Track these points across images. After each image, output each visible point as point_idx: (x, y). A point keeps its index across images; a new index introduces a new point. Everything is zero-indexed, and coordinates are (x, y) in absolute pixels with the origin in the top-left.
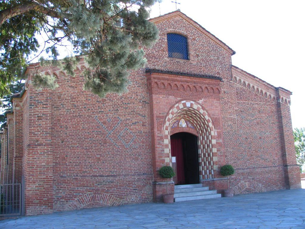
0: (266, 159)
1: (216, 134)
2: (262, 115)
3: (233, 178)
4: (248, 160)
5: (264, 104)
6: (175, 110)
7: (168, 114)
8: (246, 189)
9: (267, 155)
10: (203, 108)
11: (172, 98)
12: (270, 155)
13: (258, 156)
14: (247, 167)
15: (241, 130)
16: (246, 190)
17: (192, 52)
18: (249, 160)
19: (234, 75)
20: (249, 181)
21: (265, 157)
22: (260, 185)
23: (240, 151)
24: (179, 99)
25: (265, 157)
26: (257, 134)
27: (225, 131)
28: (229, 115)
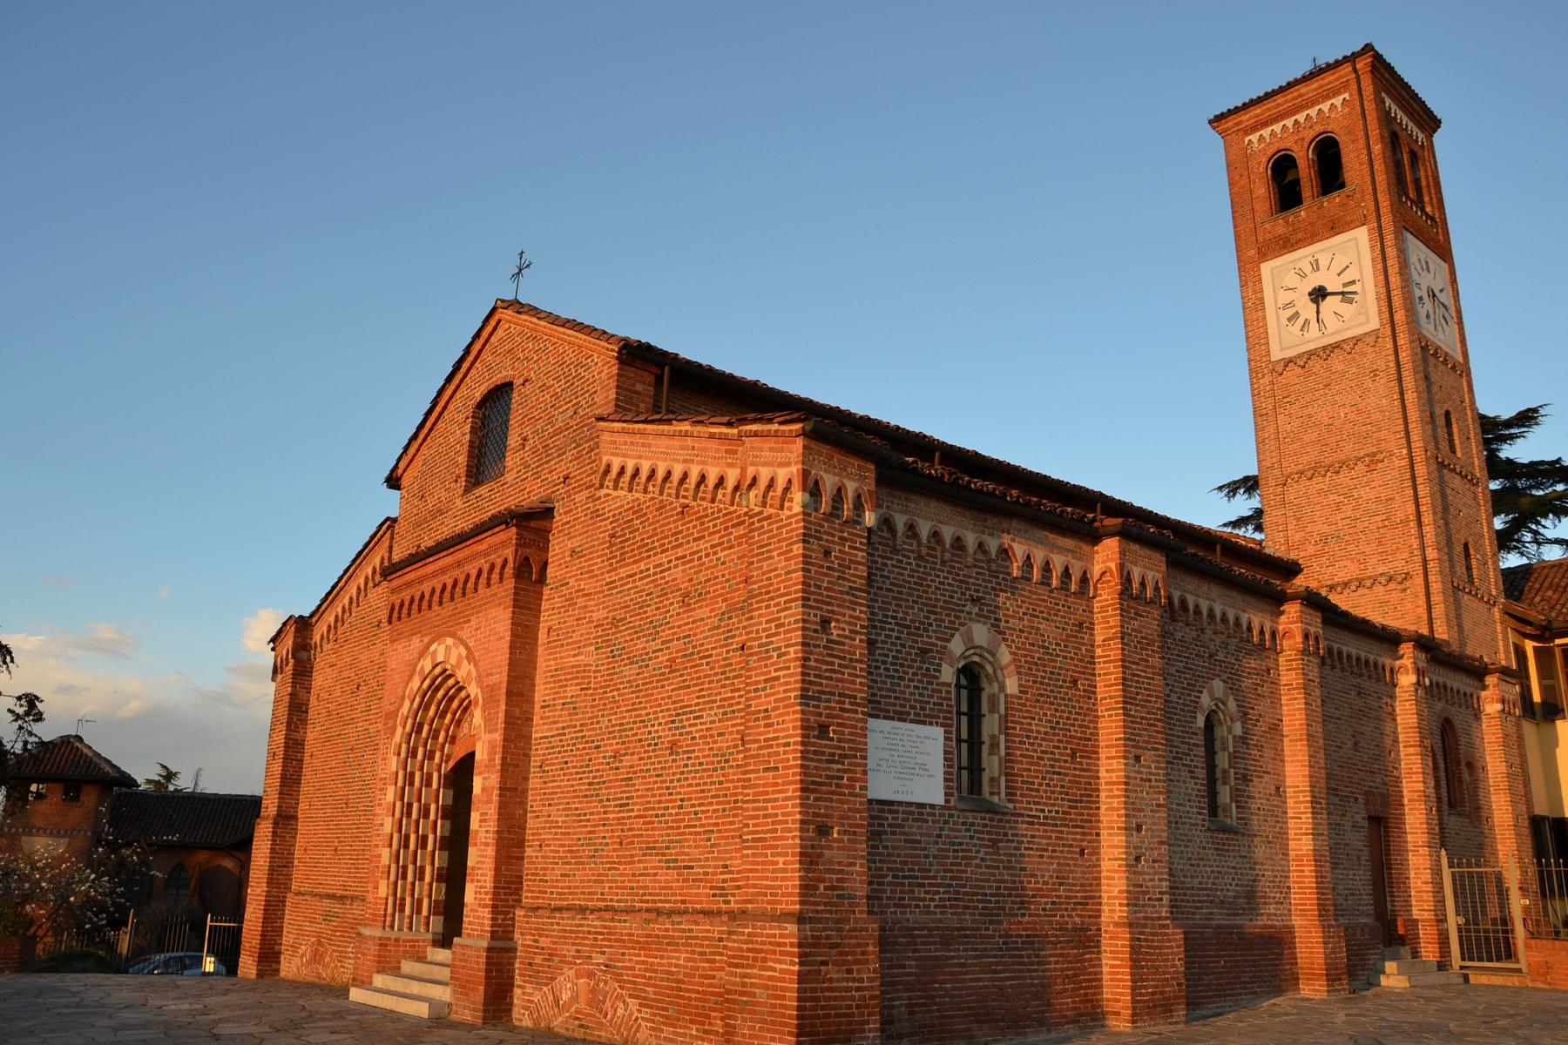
0: (686, 867)
1: (485, 757)
2: (700, 613)
3: (543, 948)
4: (610, 869)
5: (713, 546)
6: (416, 683)
7: (403, 698)
8: (576, 1012)
9: (695, 841)
10: (470, 657)
11: (416, 643)
12: (709, 840)
13: (650, 849)
14: (605, 900)
15: (603, 716)
16: (577, 1019)
17: (513, 441)
18: (616, 869)
19: (606, 454)
20: (590, 975)
21: (683, 854)
22: (633, 1004)
23: (588, 820)
24: (426, 639)
25: (683, 854)
26: (660, 724)
27: (551, 730)
28: (574, 656)
